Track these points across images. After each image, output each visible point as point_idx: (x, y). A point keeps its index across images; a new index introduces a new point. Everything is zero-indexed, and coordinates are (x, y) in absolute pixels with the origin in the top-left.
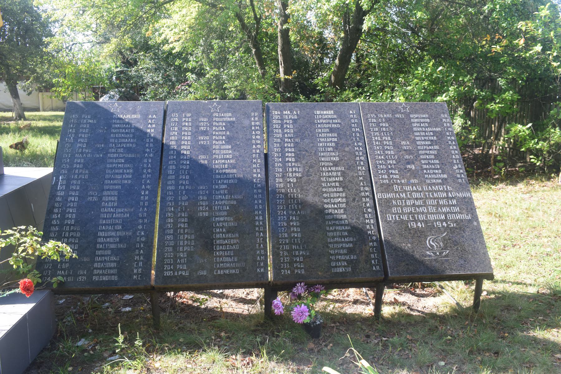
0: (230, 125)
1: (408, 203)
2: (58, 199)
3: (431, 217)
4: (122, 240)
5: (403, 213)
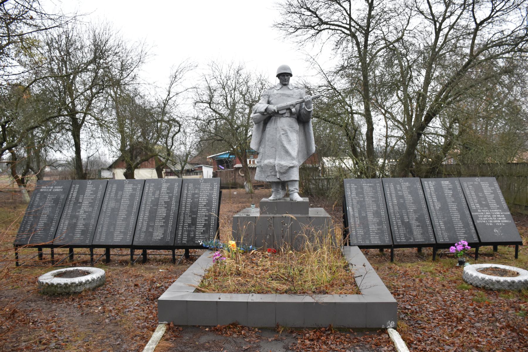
0: (408, 187)
1: (485, 216)
2: (351, 215)
3: (495, 221)
4: (378, 229)
5: (484, 220)
